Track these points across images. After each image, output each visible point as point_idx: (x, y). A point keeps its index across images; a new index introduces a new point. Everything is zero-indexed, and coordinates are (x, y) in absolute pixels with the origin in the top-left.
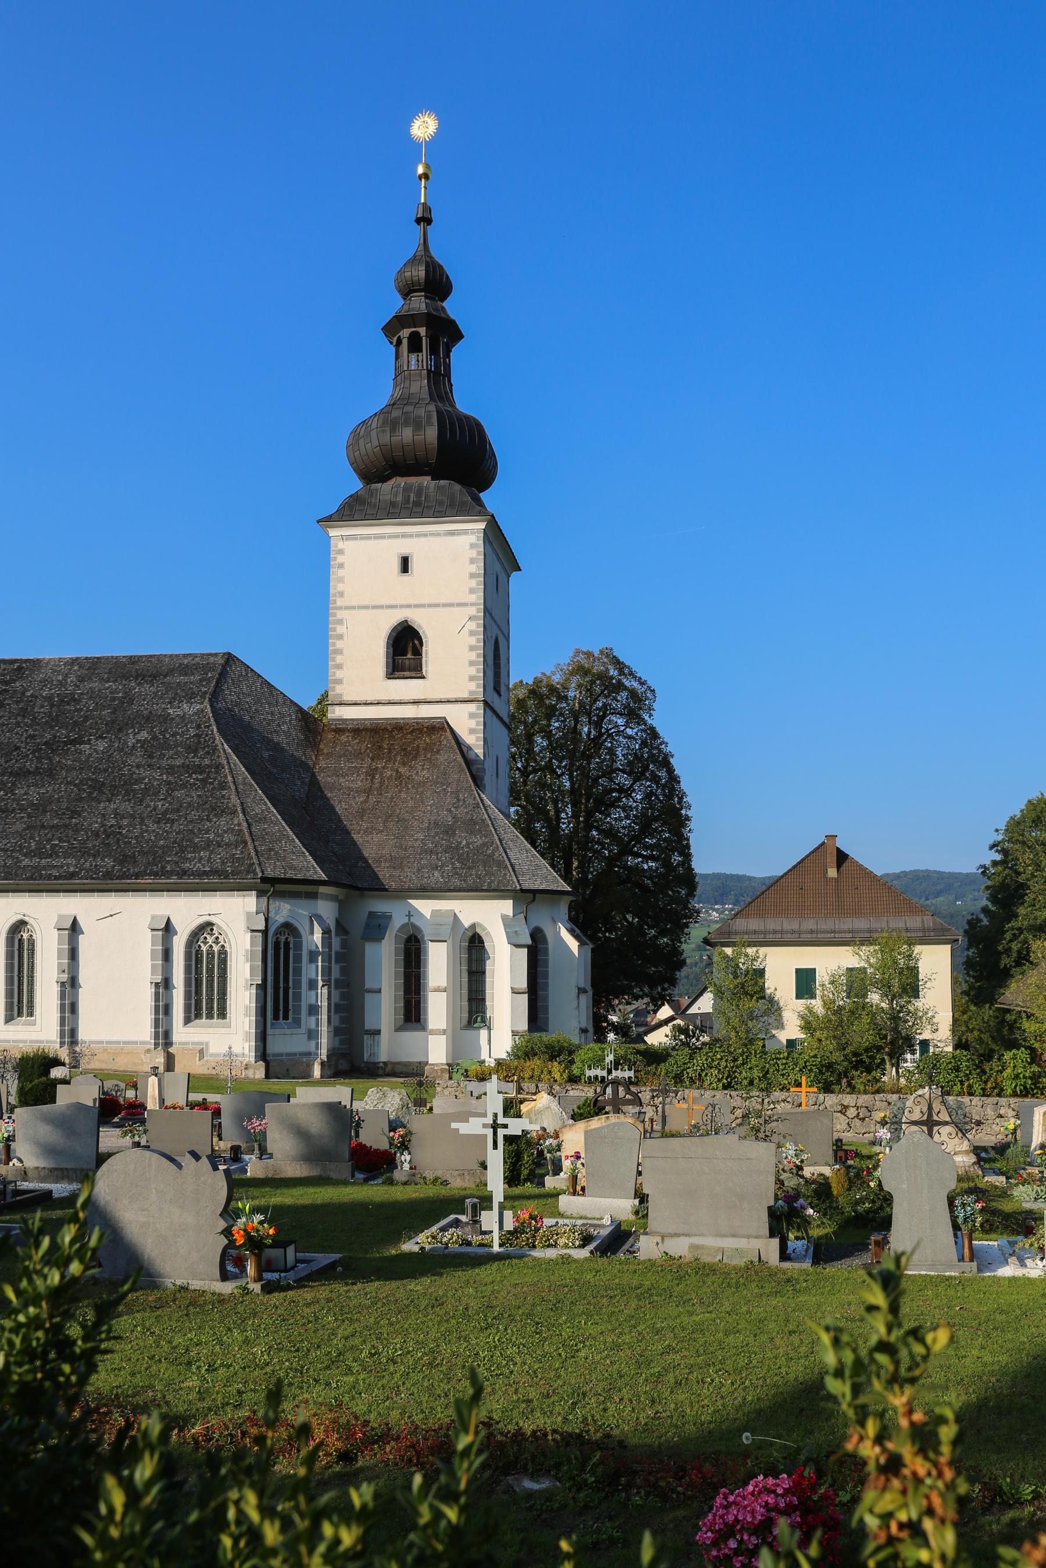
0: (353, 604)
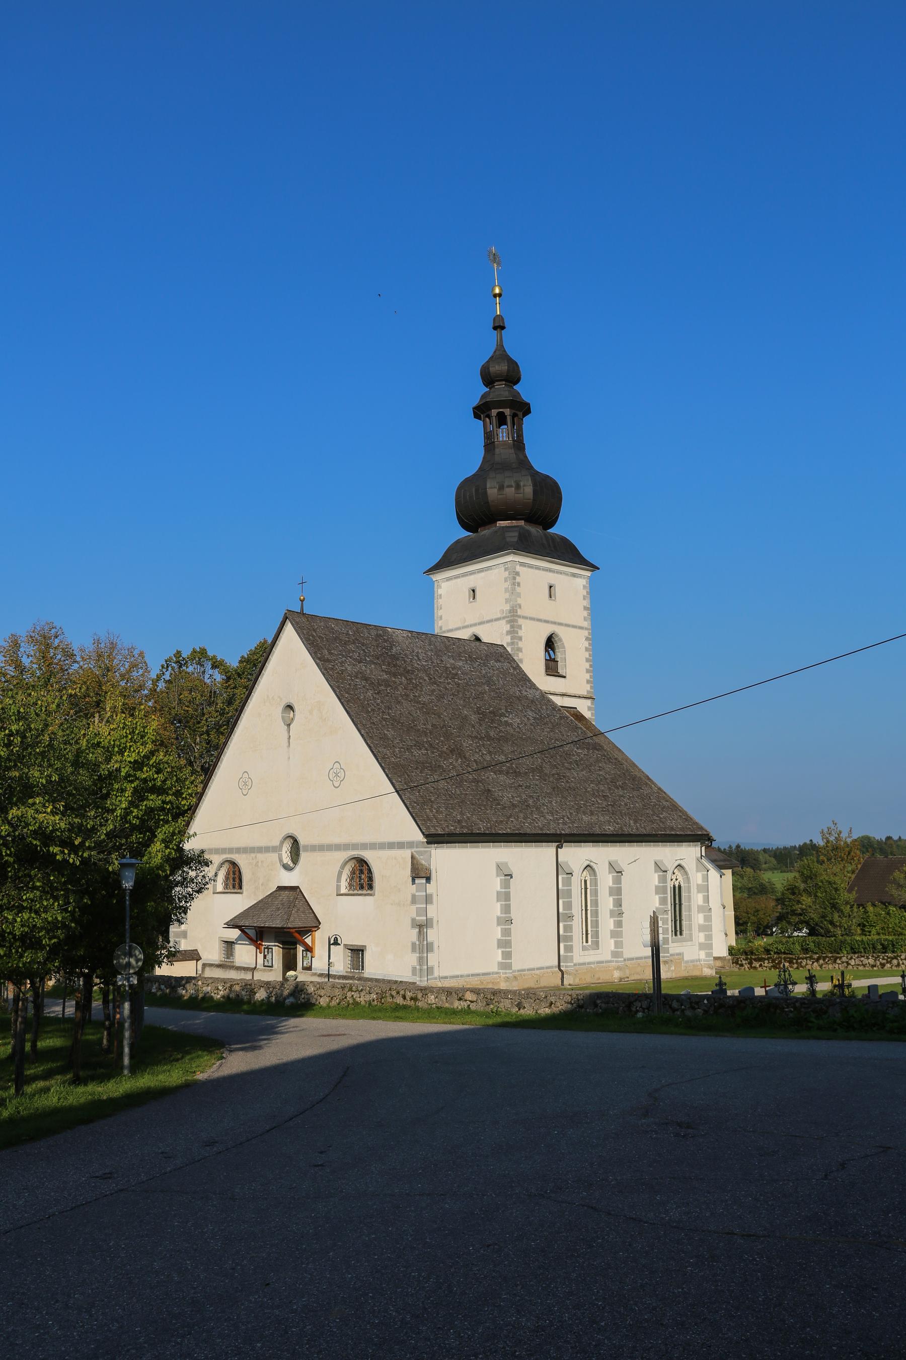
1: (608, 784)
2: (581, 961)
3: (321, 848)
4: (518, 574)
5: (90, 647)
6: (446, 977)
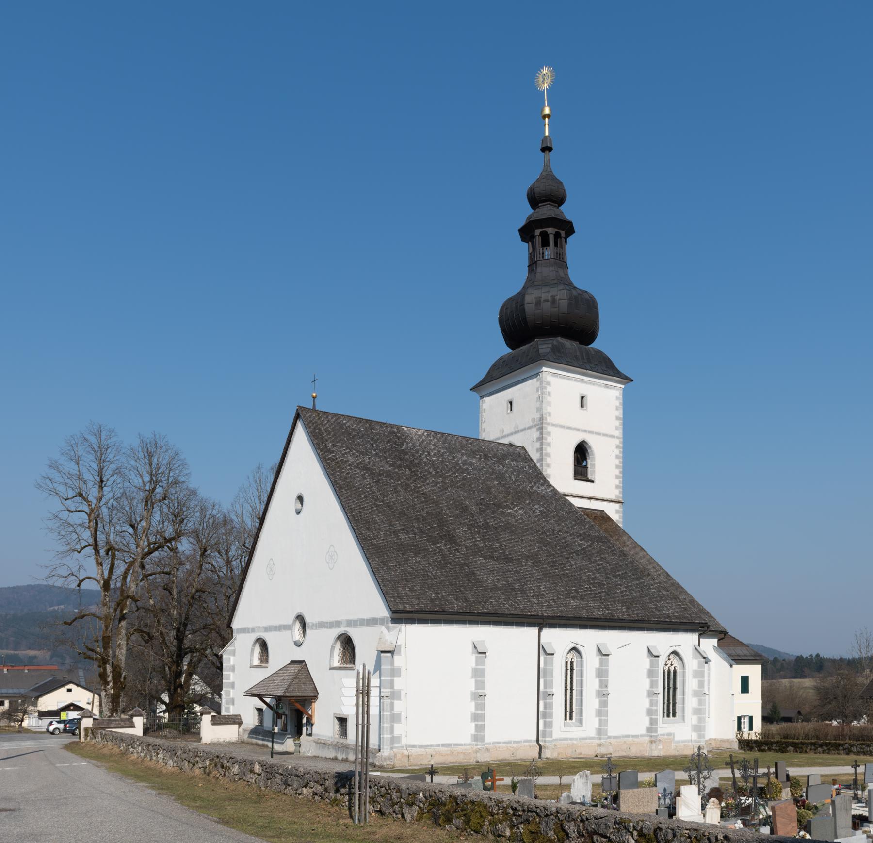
0: (556, 422)
1: (606, 573)
2: (563, 736)
3: (320, 625)
4: (549, 384)
5: (136, 443)
6: (414, 747)
